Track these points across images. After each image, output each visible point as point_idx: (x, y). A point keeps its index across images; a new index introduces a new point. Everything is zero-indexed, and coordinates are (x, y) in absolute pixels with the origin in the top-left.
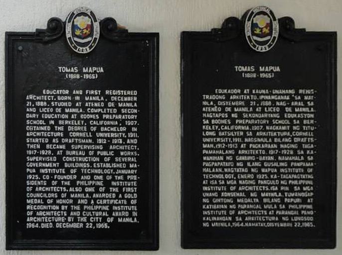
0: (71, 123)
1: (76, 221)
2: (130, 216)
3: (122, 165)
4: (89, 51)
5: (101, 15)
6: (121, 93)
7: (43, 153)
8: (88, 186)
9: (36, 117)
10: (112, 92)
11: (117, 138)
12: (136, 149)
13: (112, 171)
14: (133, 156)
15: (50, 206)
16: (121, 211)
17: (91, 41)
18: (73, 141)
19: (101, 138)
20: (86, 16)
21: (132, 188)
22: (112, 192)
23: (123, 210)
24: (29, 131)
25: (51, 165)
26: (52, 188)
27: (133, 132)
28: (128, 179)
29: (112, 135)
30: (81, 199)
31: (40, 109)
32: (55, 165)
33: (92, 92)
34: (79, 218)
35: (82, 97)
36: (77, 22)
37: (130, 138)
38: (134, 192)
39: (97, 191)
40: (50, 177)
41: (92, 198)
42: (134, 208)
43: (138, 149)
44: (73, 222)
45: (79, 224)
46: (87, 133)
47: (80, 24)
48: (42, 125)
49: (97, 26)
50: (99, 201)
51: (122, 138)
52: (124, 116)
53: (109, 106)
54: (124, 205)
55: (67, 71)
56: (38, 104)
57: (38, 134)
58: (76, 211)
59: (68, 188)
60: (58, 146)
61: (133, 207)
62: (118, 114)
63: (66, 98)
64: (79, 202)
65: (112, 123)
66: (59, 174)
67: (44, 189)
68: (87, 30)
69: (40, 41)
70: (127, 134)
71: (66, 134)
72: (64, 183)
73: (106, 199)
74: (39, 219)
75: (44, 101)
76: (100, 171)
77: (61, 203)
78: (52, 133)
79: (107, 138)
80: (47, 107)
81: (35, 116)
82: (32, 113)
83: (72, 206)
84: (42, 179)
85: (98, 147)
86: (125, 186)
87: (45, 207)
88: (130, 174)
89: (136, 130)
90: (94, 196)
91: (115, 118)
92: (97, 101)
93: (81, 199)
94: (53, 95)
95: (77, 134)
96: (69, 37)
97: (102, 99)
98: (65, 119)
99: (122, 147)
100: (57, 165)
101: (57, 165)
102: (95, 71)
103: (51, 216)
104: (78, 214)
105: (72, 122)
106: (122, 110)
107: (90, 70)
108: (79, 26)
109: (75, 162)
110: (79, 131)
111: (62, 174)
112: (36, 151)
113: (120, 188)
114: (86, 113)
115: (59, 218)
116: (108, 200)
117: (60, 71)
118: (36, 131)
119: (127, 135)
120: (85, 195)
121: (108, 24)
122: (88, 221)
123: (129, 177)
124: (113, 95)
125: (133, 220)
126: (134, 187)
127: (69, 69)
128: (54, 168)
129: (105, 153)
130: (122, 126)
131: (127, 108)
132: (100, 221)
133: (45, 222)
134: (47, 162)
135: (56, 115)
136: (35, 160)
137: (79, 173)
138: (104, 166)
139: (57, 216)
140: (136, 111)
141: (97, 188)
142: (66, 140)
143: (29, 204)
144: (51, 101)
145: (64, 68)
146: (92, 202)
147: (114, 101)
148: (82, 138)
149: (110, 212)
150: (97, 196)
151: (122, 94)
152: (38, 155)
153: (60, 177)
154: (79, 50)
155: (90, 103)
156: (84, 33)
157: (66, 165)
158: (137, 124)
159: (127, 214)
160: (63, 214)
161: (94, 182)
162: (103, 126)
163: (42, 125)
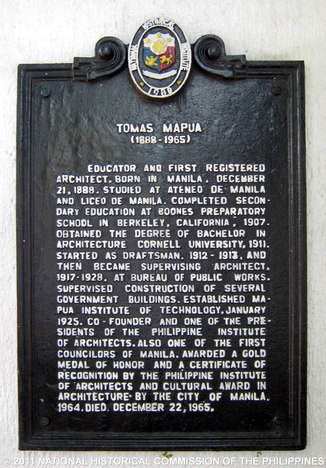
0: (140, 223)
1: (150, 399)
2: (253, 389)
3: (238, 298)
4: (171, 93)
5: (194, 33)
6: (235, 168)
7: (89, 279)
8: (174, 337)
9: (74, 212)
10: (218, 167)
11: (228, 250)
12: (263, 268)
13: (218, 309)
14: (259, 282)
15: (100, 374)
16: (235, 381)
17: (176, 75)
18: (144, 256)
19: (198, 250)
20: (165, 33)
21: (256, 340)
22: (219, 348)
23: (240, 380)
24: (62, 239)
25: (102, 300)
26: (105, 341)
27: (258, 239)
28: (249, 323)
29: (219, 244)
30: (159, 359)
31: (82, 199)
32: (109, 299)
33: (181, 168)
34: (156, 394)
35: (162, 175)
36: (149, 41)
37: (253, 250)
38: (261, 347)
39: (190, 346)
40: (101, 322)
41: (181, 359)
42: (260, 375)
43: (268, 269)
44: (145, 402)
45: (155, 404)
46: (171, 242)
47: (154, 47)
48: (86, 228)
49: (185, 50)
50: (193, 364)
51: (237, 249)
52: (240, 209)
53: (212, 192)
54: (241, 370)
55: (133, 130)
56: (79, 190)
57: (79, 244)
58: (150, 381)
59: (134, 340)
60: (115, 265)
61: (258, 373)
62: (228, 206)
63: (130, 179)
64: (156, 365)
65: (218, 222)
66: (119, 315)
67: (90, 343)
68: (168, 56)
69: (82, 79)
70: (246, 243)
71: (131, 243)
72: (127, 331)
73: (207, 360)
74: (81, 397)
75: (89, 185)
76: (195, 310)
77: (122, 367)
78: (105, 242)
79: (209, 250)
80: (94, 195)
81: (72, 212)
82: (67, 206)
83: (143, 374)
84: (85, 325)
85: (191, 266)
86: (243, 337)
87: (91, 375)
88: (253, 315)
89: (264, 235)
90: (185, 354)
91: (223, 213)
92: (189, 184)
93: (159, 359)
94: (106, 173)
95: (153, 244)
96: (135, 69)
97: (199, 179)
98: (129, 217)
99: (237, 266)
100: (114, 299)
101: (114, 299)
102: (186, 130)
103: (103, 391)
104: (154, 386)
105: (143, 223)
106: (237, 199)
107: (177, 129)
108: (152, 49)
109: (147, 295)
110: (155, 238)
111: (123, 316)
112: (74, 275)
113: (234, 339)
114: (170, 205)
115: (118, 394)
116: (211, 362)
117: (120, 131)
118: (72, 239)
119: (248, 245)
120: (168, 354)
121: (209, 49)
122: (174, 399)
123: (250, 320)
124: (219, 173)
125: (259, 396)
126: (260, 337)
127: (137, 128)
128: (108, 304)
129: (205, 277)
130: (238, 228)
131: (247, 195)
132: (197, 399)
133: (92, 402)
134: (96, 294)
135: (111, 210)
136: (73, 290)
137: (156, 312)
138: (204, 300)
139: (115, 391)
140: (263, 200)
141: (190, 341)
142: (132, 255)
143: (61, 370)
144: (103, 184)
145: (128, 125)
146: (181, 365)
147: (222, 183)
148: (161, 250)
149: (215, 383)
150: (191, 354)
151: (237, 170)
152: (78, 281)
153: (119, 322)
154: (152, 93)
155: (176, 188)
156: (162, 61)
157: (131, 300)
158: (265, 223)
159: (247, 386)
160: (127, 387)
161: (183, 331)
162: (202, 227)
163: (86, 228)
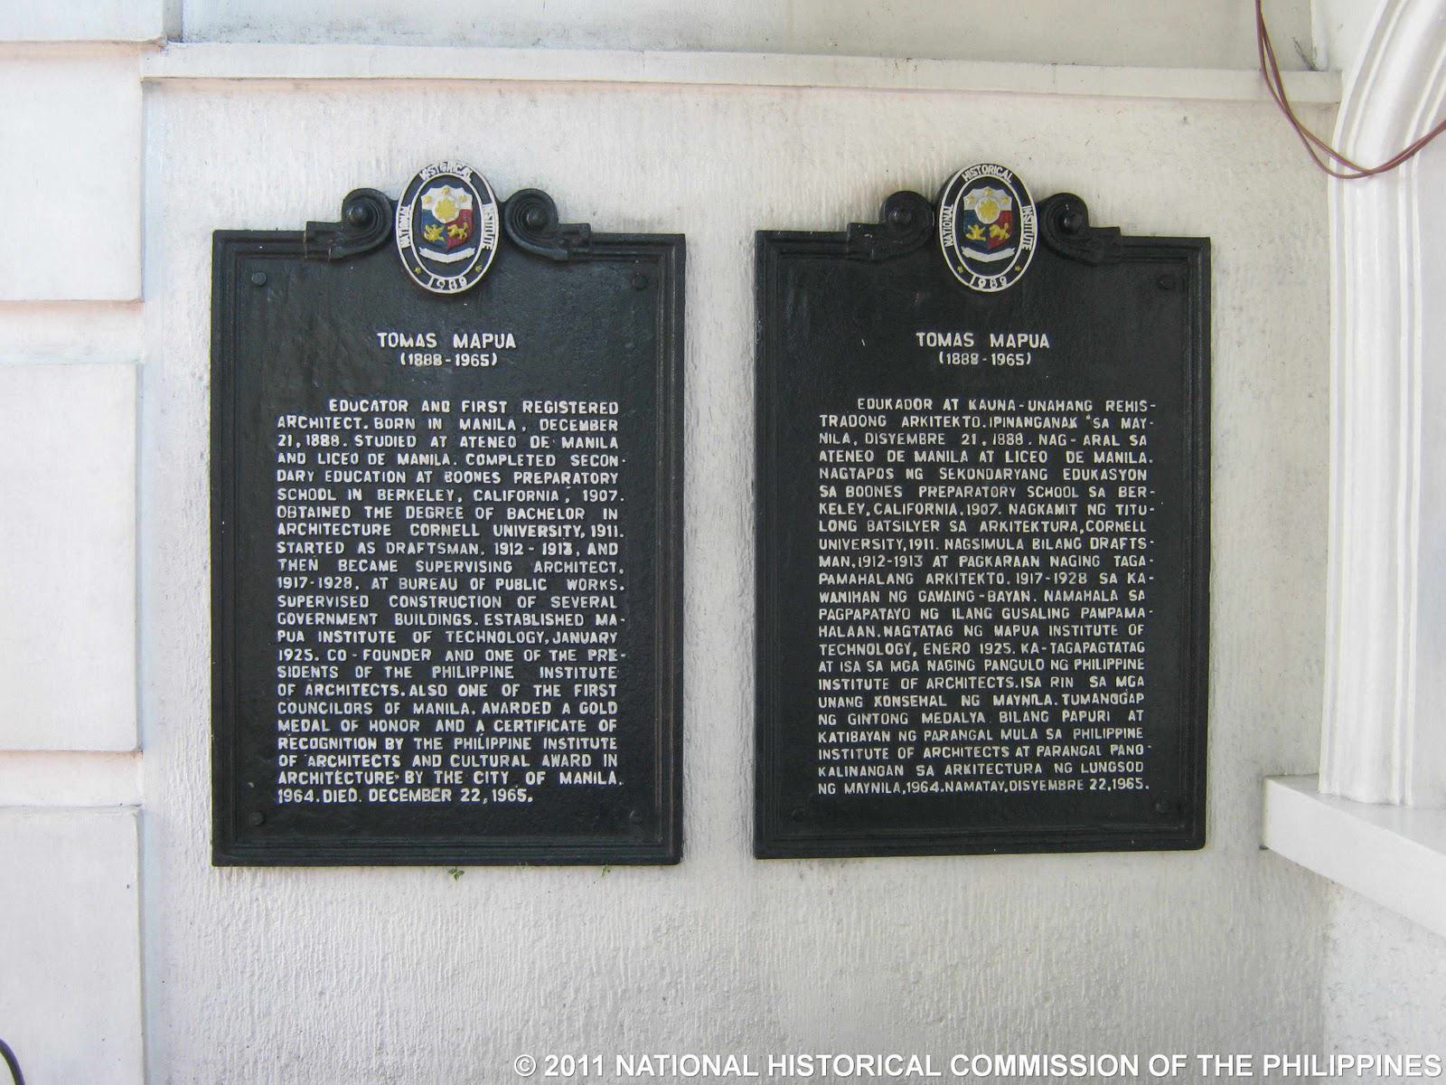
1: (428, 780)
2: (597, 765)
3: (573, 618)
6: (570, 407)
7: (330, 585)
8: (468, 681)
9: (307, 476)
10: (542, 405)
11: (557, 540)
13: (540, 636)
14: (607, 593)
15: (348, 740)
16: (568, 752)
18: (420, 549)
19: (508, 539)
21: (602, 686)
22: (542, 698)
23: (575, 750)
26: (356, 686)
27: (606, 523)
28: (590, 659)
30: (444, 717)
31: (320, 455)
32: (363, 619)
33: (481, 406)
35: (451, 419)
37: (597, 540)
38: (609, 698)
39: (494, 694)
42: (608, 743)
43: (621, 571)
44: (421, 786)
45: (437, 790)
46: (464, 526)
48: (326, 503)
51: (572, 538)
52: (577, 475)
53: (532, 446)
54: (576, 734)
55: (403, 343)
56: (314, 440)
57: (313, 529)
58: (429, 752)
59: (404, 684)
60: (373, 563)
61: (604, 740)
62: (557, 469)
64: (439, 726)
65: (541, 495)
66: (378, 645)
70: (586, 529)
71: (400, 528)
73: (524, 717)
74: (315, 778)
75: (331, 432)
76: (502, 637)
78: (356, 526)
79: (526, 541)
80: (340, 449)
81: (302, 477)
82: (293, 467)
83: (418, 740)
84: (323, 661)
85: (496, 566)
86: (580, 680)
88: (597, 646)
90: (486, 708)
92: (495, 433)
93: (444, 717)
94: (359, 413)
95: (435, 529)
97: (511, 424)
98: (396, 485)
100: (370, 619)
101: (370, 619)
103: (353, 769)
105: (419, 495)
106: (573, 458)
107: (475, 343)
109: (425, 612)
110: (438, 521)
111: (386, 646)
112: (305, 579)
113: (566, 685)
114: (463, 467)
115: (377, 773)
116: (529, 722)
118: (303, 520)
120: (458, 708)
122: (467, 782)
123: (592, 653)
124: (544, 415)
126: (607, 681)
128: (362, 627)
129: (519, 584)
131: (589, 451)
132: (505, 782)
133: (333, 787)
135: (368, 473)
136: (304, 604)
137: (439, 642)
138: (517, 620)
139: (371, 769)
140: (614, 461)
141: (494, 686)
142: (401, 547)
143: (284, 734)
144: (354, 431)
145: (395, 334)
146: (480, 726)
147: (548, 432)
148: (449, 540)
149: (535, 756)
150: (495, 709)
151: (573, 412)
152: (312, 590)
153: (379, 656)
155: (473, 439)
157: (399, 620)
159: (586, 761)
160: (391, 761)
161: (484, 670)
162: (514, 503)
163: (326, 503)
